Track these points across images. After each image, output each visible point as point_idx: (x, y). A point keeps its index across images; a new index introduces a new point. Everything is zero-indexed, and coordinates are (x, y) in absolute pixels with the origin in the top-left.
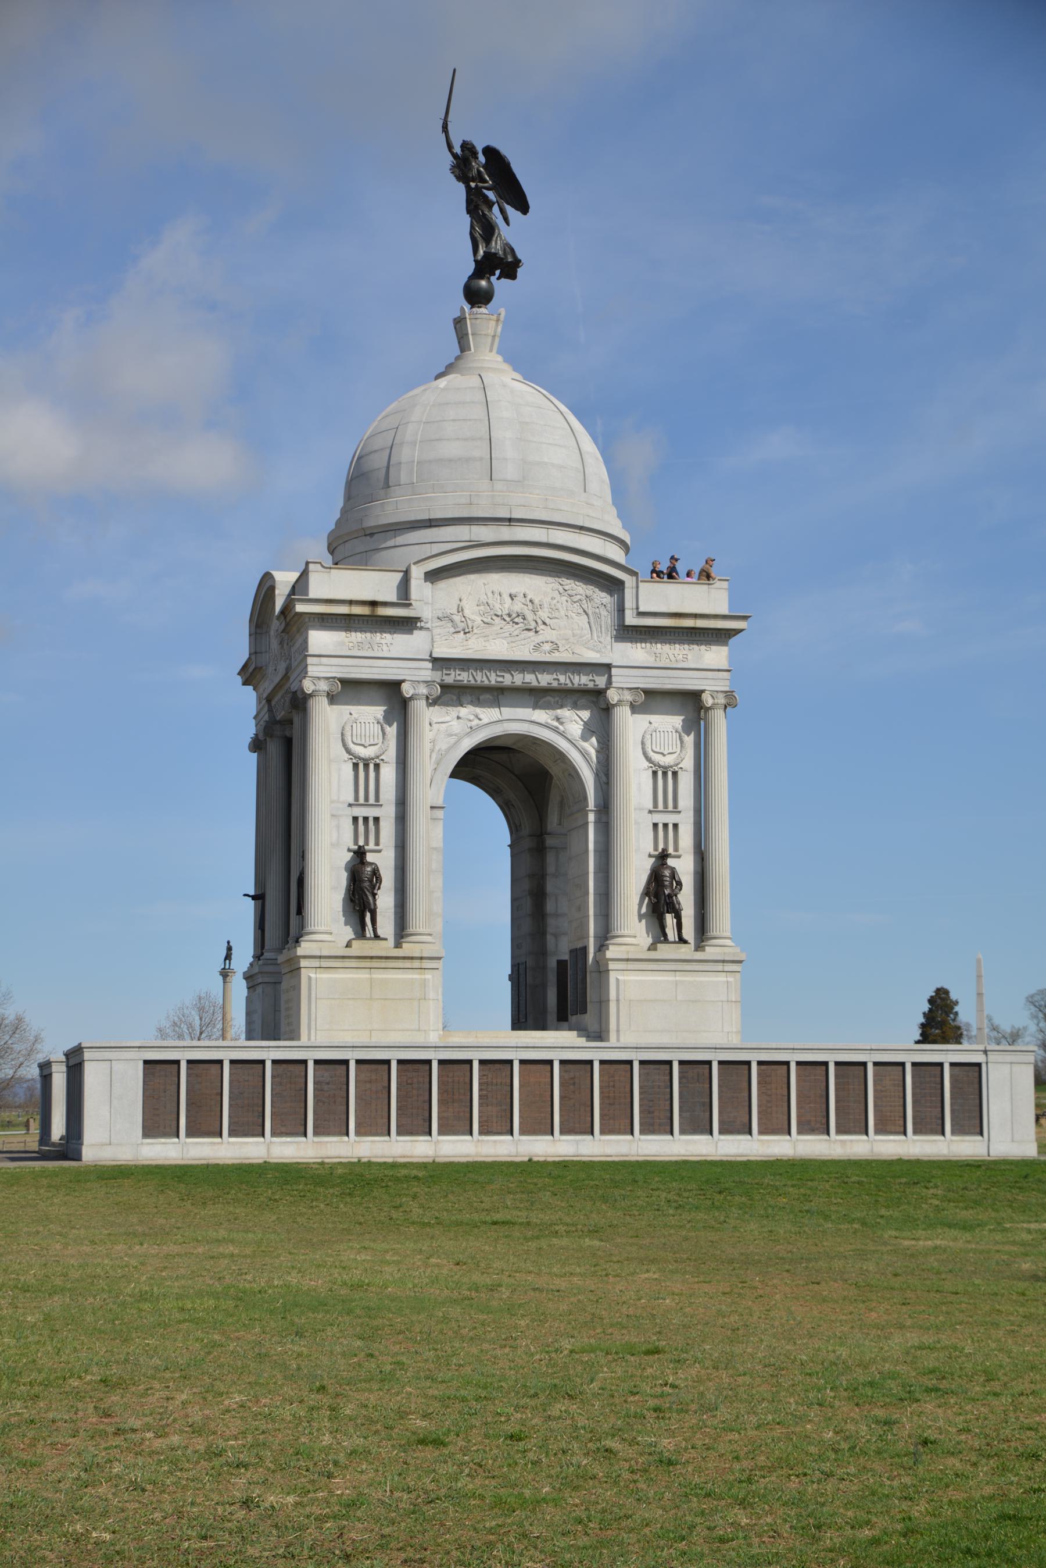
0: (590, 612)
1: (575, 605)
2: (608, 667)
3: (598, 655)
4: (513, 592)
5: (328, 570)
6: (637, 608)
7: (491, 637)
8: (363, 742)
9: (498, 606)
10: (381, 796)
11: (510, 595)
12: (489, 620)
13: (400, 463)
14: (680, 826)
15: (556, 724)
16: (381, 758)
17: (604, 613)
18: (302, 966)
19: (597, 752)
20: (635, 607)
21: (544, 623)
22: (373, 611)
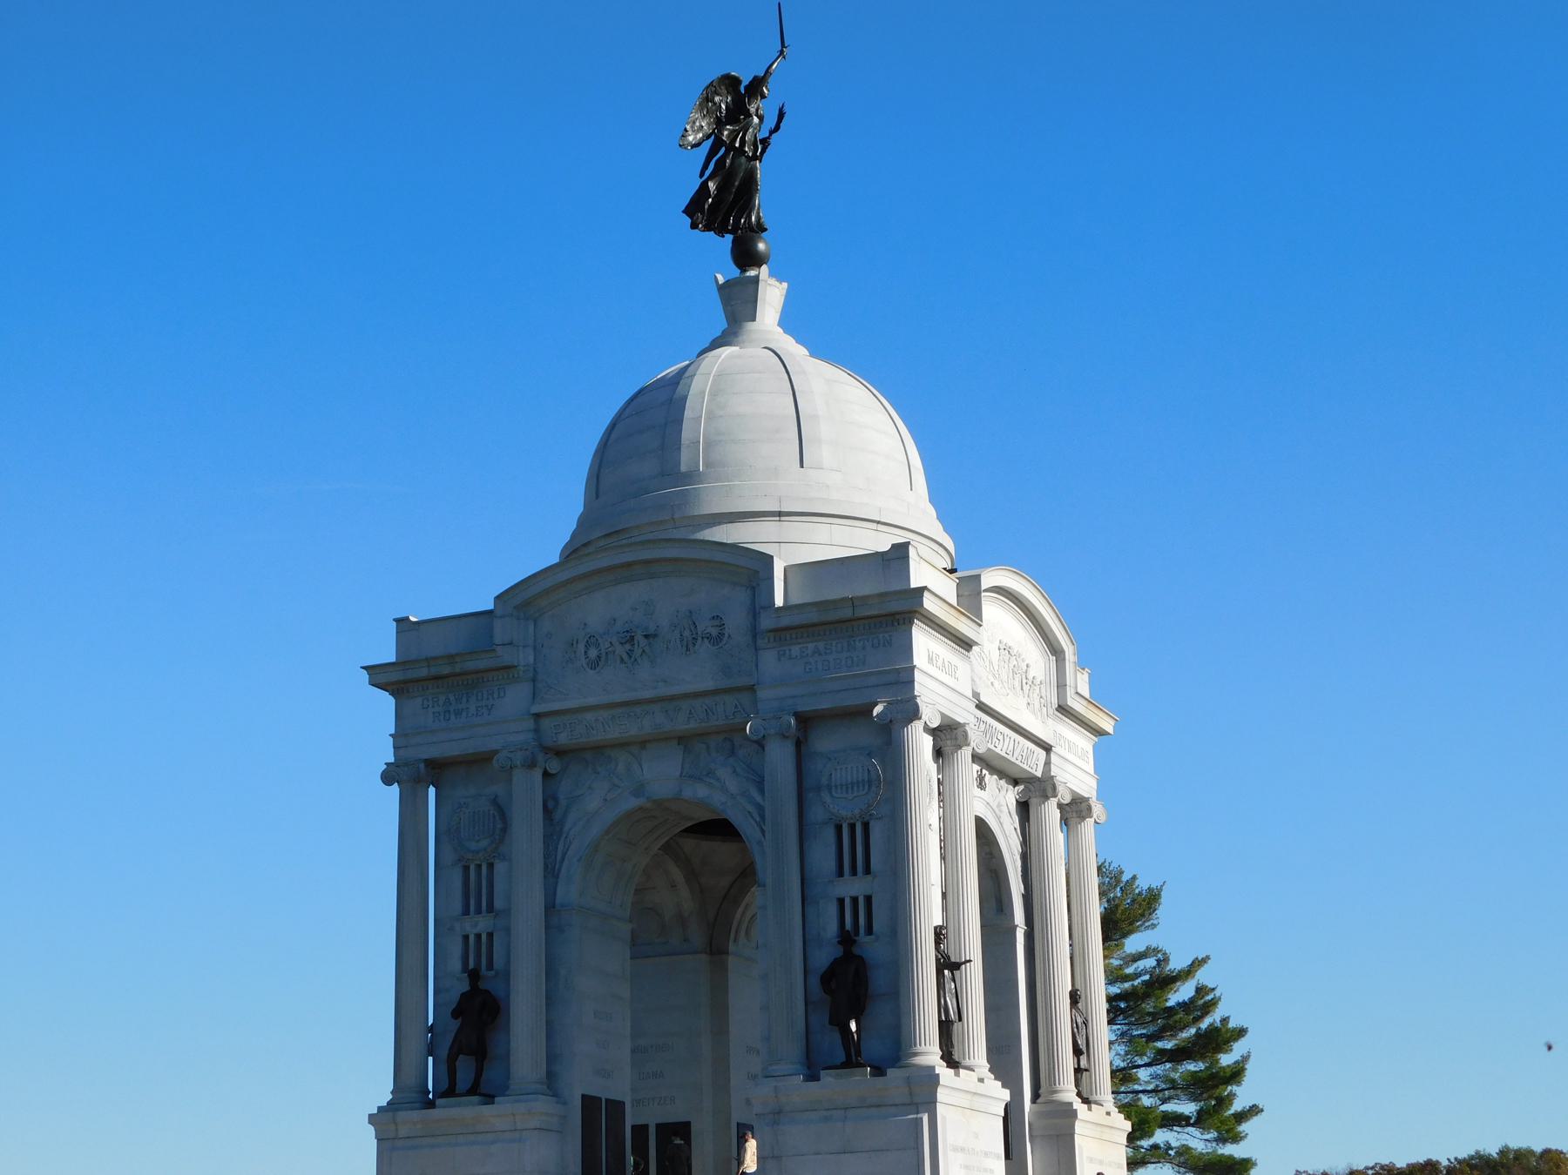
2: (1048, 748)
6: (1076, 687)
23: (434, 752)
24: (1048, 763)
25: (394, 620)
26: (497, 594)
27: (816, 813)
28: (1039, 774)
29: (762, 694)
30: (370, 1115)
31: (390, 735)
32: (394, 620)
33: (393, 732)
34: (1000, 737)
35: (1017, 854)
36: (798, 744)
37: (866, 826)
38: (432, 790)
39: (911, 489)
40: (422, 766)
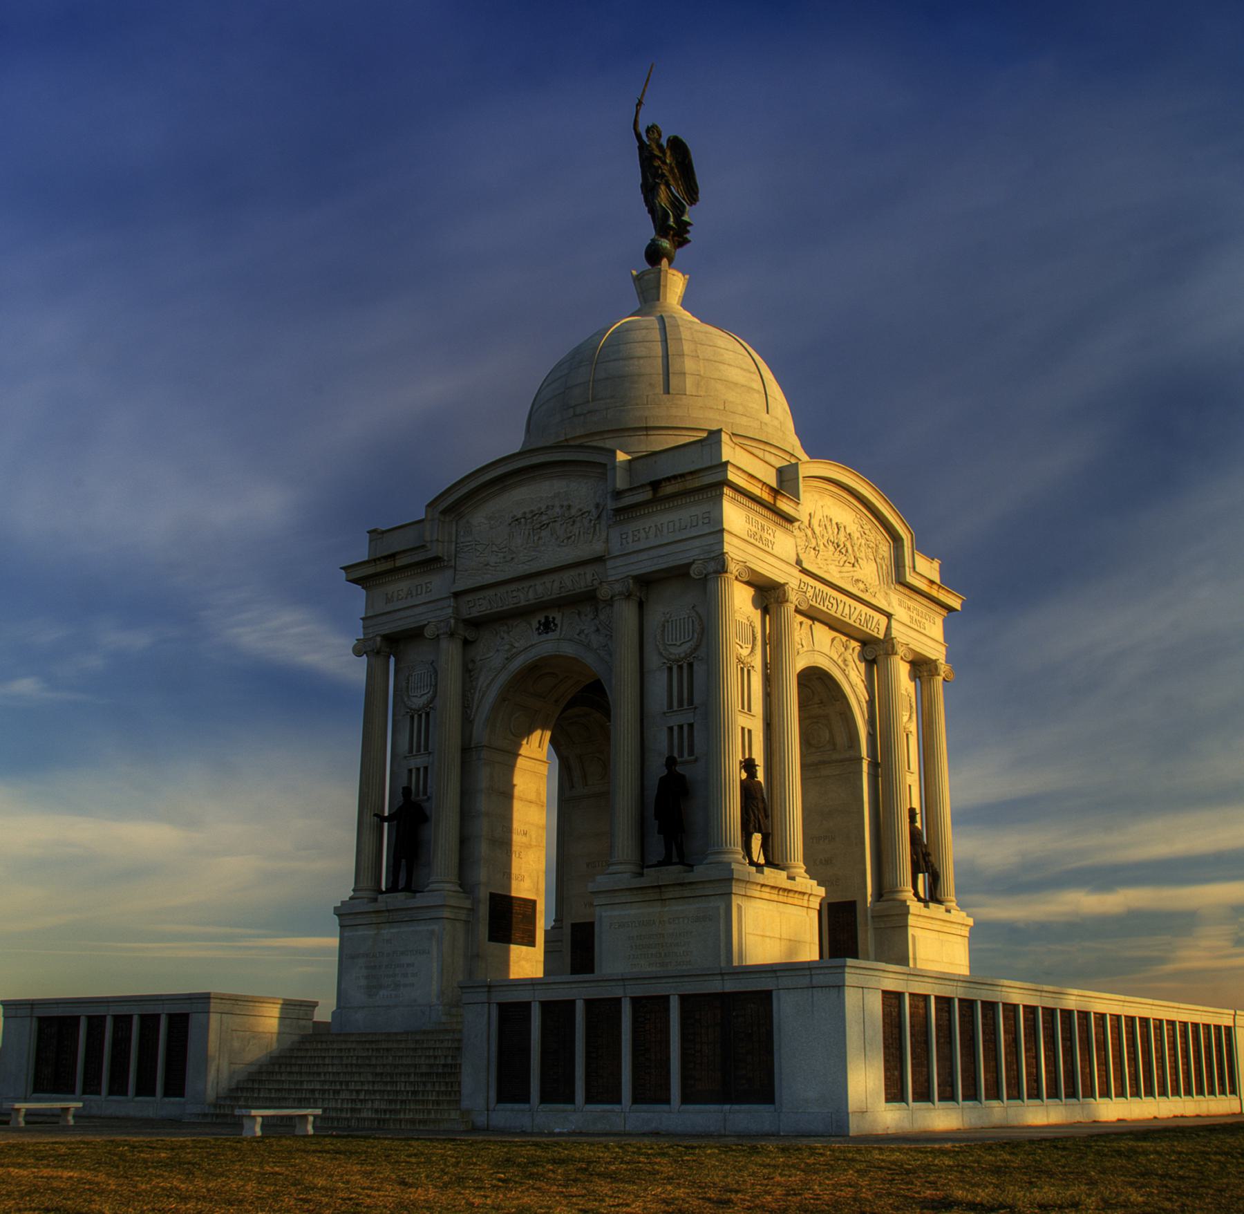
0: (878, 560)
1: (870, 550)
2: (889, 616)
3: (885, 603)
4: (839, 521)
5: (733, 445)
7: (829, 562)
8: (740, 643)
9: (830, 532)
10: (752, 708)
11: (837, 524)
12: (826, 543)
13: (685, 373)
14: (912, 787)
15: (843, 666)
16: (752, 664)
17: (884, 567)
18: (734, 892)
19: (867, 702)
20: (911, 566)
21: (857, 561)
22: (775, 501)
23: (387, 629)
24: (888, 628)
25: (368, 532)
26: (426, 504)
27: (653, 661)
28: (881, 636)
29: (610, 564)
30: (336, 908)
31: (361, 619)
32: (368, 532)
33: (363, 616)
34: (834, 602)
35: (864, 701)
36: (641, 605)
37: (691, 665)
38: (392, 659)
39: (768, 413)
40: (379, 639)
